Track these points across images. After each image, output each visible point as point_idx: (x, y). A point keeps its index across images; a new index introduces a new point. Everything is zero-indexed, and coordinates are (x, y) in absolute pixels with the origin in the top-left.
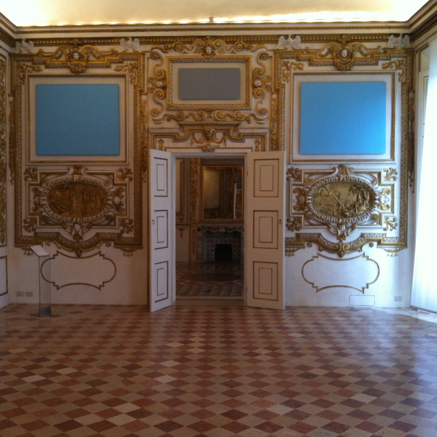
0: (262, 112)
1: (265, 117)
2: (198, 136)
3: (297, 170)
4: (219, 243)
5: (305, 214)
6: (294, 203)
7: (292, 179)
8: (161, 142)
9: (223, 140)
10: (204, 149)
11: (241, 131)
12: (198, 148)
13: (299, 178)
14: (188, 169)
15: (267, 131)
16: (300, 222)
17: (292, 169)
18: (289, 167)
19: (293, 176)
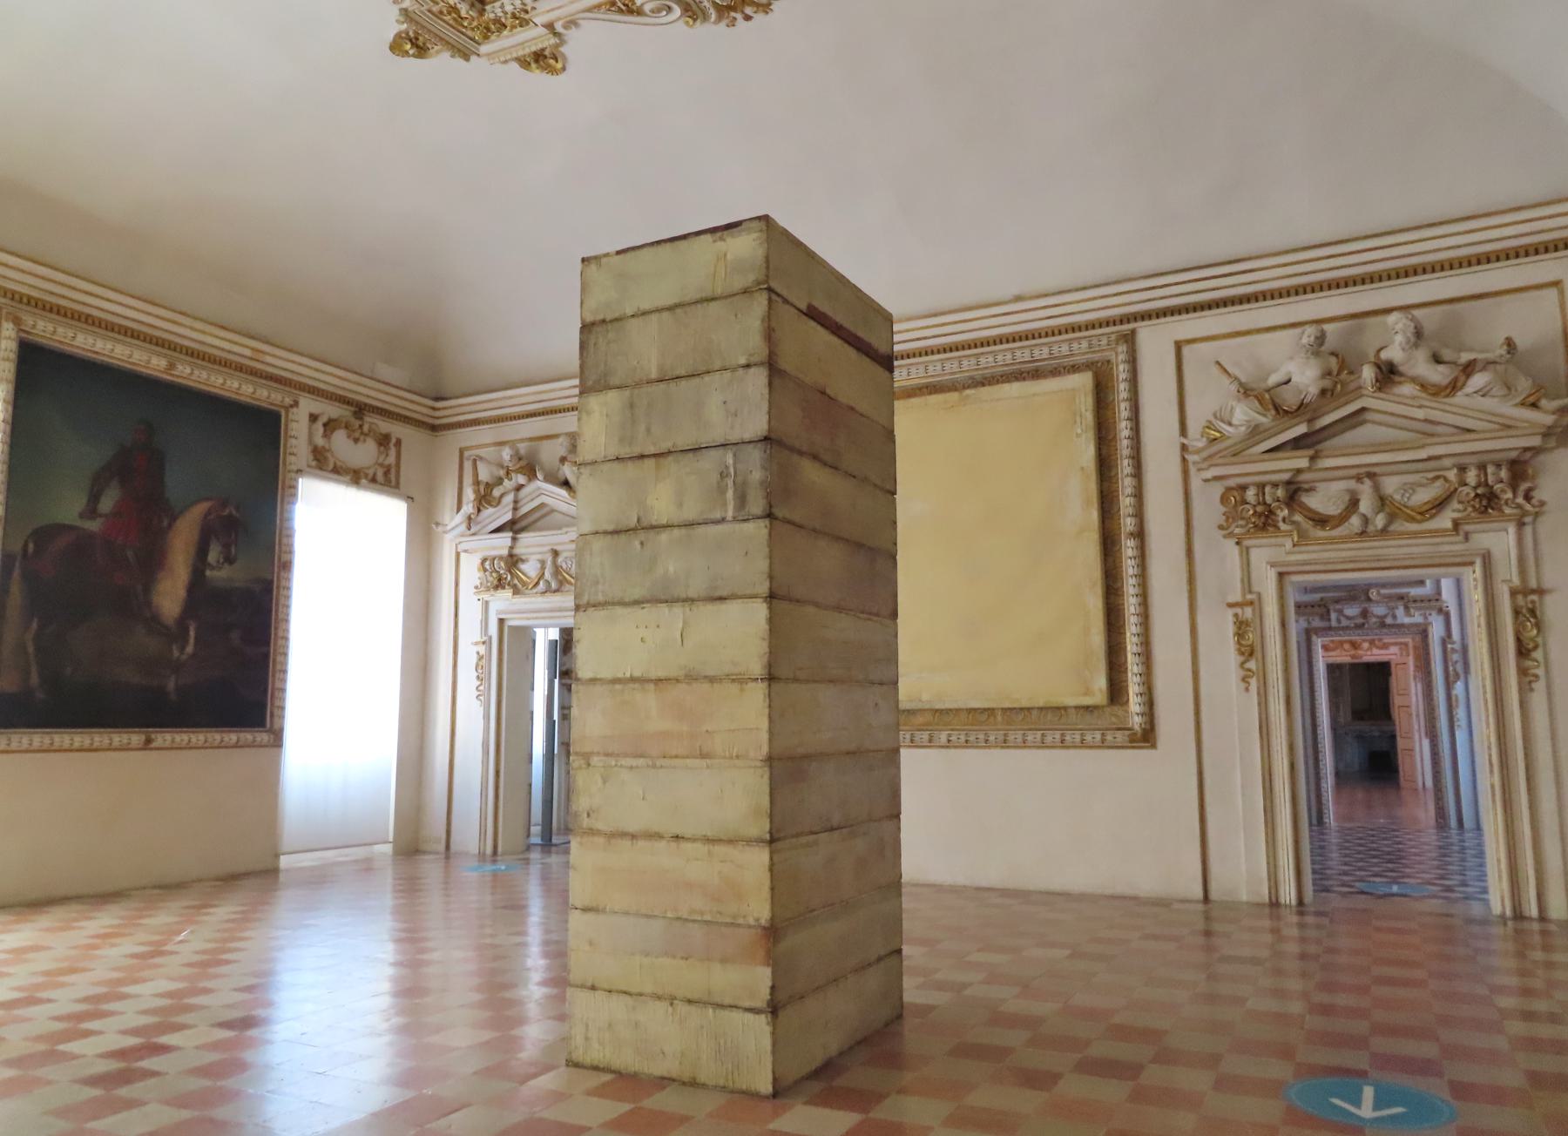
9: (1370, 649)
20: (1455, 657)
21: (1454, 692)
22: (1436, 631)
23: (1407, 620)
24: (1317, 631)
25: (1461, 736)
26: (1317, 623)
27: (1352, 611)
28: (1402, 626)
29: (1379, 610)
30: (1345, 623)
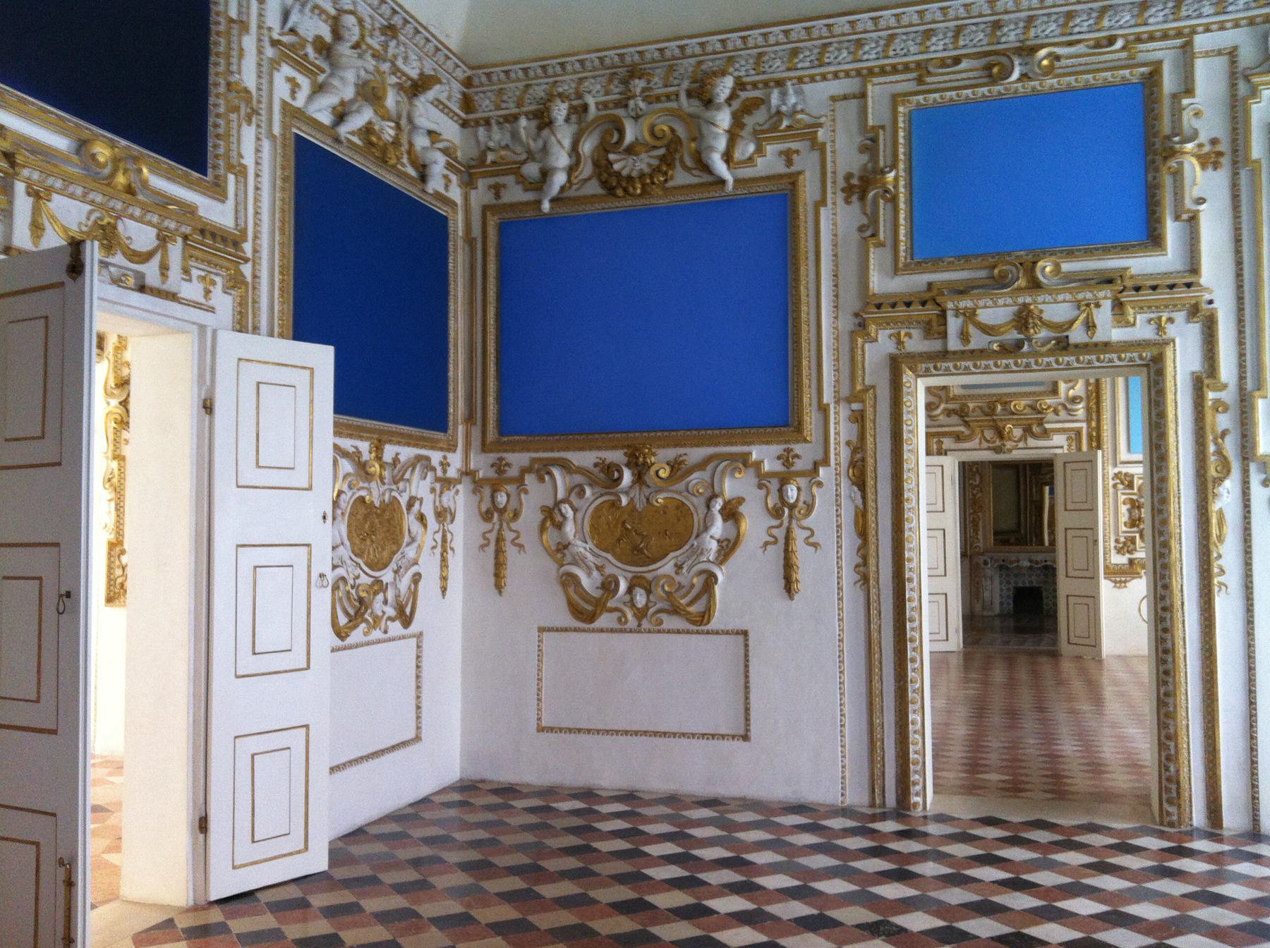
0: (1074, 400)
1: (1080, 406)
2: (989, 434)
3: (1126, 474)
4: (1020, 585)
6: (1124, 516)
7: (1120, 487)
9: (1023, 438)
11: (1047, 426)
12: (989, 449)
13: (1130, 486)
15: (1084, 425)
17: (1120, 473)
18: (1116, 470)
19: (1122, 483)
20: (1224, 421)
21: (1215, 506)
22: (1183, 359)
23: (1117, 335)
24: (914, 360)
25: (1226, 608)
26: (916, 343)
27: (996, 312)
28: (1106, 346)
29: (1056, 310)
30: (978, 340)
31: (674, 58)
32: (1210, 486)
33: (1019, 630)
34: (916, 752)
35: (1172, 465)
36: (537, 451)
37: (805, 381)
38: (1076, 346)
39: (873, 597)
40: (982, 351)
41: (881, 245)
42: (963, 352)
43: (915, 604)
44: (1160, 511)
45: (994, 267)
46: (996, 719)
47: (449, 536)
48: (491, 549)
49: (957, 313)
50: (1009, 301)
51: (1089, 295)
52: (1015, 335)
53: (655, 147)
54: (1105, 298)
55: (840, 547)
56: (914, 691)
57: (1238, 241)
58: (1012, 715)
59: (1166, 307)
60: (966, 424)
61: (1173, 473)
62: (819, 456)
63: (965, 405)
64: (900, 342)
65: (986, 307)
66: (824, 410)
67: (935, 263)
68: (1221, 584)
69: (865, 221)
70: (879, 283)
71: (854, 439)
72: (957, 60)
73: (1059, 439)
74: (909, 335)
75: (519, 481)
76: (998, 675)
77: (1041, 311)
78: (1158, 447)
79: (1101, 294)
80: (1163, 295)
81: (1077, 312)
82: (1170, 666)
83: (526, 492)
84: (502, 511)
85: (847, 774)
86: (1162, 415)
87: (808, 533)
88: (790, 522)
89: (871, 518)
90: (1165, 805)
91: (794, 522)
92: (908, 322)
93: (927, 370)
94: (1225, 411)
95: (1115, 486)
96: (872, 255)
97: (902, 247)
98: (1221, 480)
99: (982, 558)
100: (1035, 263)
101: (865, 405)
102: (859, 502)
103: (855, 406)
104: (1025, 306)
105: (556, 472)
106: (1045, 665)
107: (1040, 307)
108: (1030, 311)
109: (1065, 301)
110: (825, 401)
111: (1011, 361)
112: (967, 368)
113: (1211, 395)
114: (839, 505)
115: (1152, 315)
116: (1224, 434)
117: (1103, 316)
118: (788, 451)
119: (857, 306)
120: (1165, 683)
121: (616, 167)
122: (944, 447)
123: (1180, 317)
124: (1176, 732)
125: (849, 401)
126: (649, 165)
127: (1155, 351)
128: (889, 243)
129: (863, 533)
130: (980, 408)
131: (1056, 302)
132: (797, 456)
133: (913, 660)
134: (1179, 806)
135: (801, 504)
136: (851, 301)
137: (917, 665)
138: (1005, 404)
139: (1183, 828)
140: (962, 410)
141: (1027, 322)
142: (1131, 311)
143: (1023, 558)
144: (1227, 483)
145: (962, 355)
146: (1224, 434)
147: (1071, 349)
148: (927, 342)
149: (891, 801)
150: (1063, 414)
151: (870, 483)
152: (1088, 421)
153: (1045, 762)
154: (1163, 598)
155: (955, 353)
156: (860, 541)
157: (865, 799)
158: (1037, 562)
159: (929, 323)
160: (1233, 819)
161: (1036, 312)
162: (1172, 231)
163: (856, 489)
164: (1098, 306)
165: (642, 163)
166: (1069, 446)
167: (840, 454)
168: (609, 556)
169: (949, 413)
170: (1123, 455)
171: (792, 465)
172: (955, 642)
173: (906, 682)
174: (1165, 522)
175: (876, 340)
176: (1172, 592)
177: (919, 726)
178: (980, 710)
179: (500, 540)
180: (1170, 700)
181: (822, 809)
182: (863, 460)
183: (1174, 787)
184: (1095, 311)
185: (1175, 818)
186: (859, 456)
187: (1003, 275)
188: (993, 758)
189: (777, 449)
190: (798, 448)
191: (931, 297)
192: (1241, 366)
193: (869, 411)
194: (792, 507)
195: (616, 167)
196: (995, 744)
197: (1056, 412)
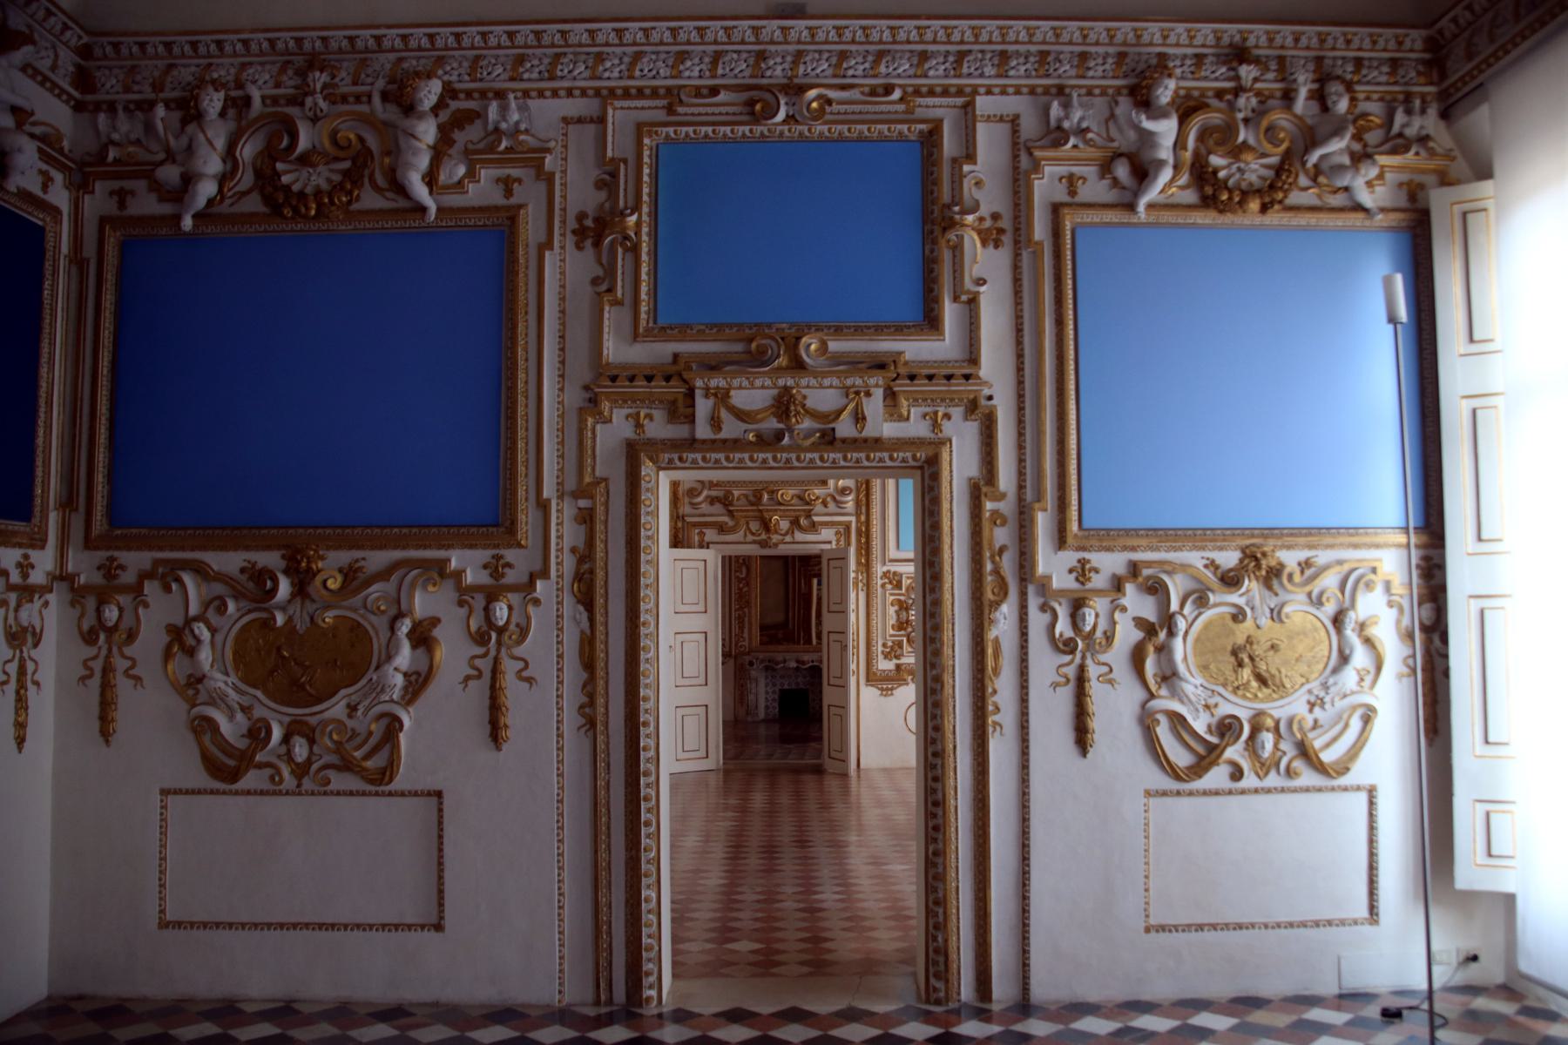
0: (844, 491)
2: (754, 526)
3: (895, 573)
5: (908, 636)
6: (892, 620)
7: (889, 586)
8: (702, 534)
9: (790, 532)
10: (764, 544)
11: (816, 519)
12: (754, 542)
13: (899, 585)
14: (736, 571)
15: (853, 519)
16: (901, 647)
20: (1001, 536)
21: (992, 634)
22: (960, 464)
23: (889, 430)
24: (655, 448)
25: (1001, 751)
26: (658, 427)
27: (752, 395)
28: (877, 443)
29: (822, 397)
30: (731, 428)
31: (367, 50)
32: (986, 611)
33: (785, 739)
34: (649, 936)
35: (947, 586)
36: (161, 549)
37: (521, 469)
38: (844, 441)
39: (601, 746)
40: (736, 441)
41: (617, 303)
42: (714, 441)
43: (652, 753)
44: (933, 640)
45: (751, 340)
46: (754, 861)
47: (30, 666)
48: (96, 682)
49: (707, 392)
50: (768, 382)
51: (859, 382)
52: (773, 424)
53: (337, 159)
54: (877, 386)
55: (560, 682)
56: (648, 862)
57: (1019, 330)
58: (770, 851)
59: (943, 400)
60: (731, 513)
61: (947, 596)
62: (538, 566)
63: (729, 492)
64: (638, 425)
65: (740, 388)
66: (544, 506)
67: (683, 331)
68: (995, 723)
69: (600, 273)
70: (615, 349)
71: (581, 545)
72: (714, 91)
73: (827, 534)
74: (650, 417)
75: (137, 590)
76: (758, 799)
77: (805, 397)
78: (932, 564)
79: (872, 381)
80: (939, 387)
81: (845, 401)
82: (940, 821)
83: (146, 605)
84: (111, 631)
85: (566, 967)
86: (936, 526)
87: (521, 665)
88: (498, 651)
89: (600, 646)
90: (933, 981)
91: (503, 650)
92: (650, 400)
93: (671, 461)
94: (1004, 524)
95: (883, 586)
96: (606, 315)
97: (644, 308)
98: (998, 604)
99: (747, 658)
100: (798, 339)
101: (594, 503)
102: (585, 624)
103: (583, 503)
104: (787, 389)
105: (187, 579)
106: (809, 780)
107: (804, 391)
108: (792, 396)
109: (831, 387)
110: (545, 495)
111: (769, 456)
112: (717, 461)
113: (989, 506)
114: (561, 630)
115: (928, 409)
116: (1002, 550)
117: (874, 406)
118: (498, 558)
119: (587, 377)
120: (935, 840)
121: (285, 179)
122: (707, 539)
123: (957, 412)
124: (945, 896)
125: (576, 495)
126: (329, 180)
127: (931, 452)
128: (628, 301)
129: (589, 663)
130: (746, 496)
131: (821, 387)
132: (508, 565)
133: (648, 824)
134: (947, 981)
135: (512, 627)
136: (580, 371)
137: (653, 829)
138: (772, 492)
139: (952, 1005)
140: (726, 497)
141: (788, 409)
142: (905, 403)
143: (789, 657)
144: (1005, 608)
145: (713, 445)
146: (1002, 550)
147: (838, 444)
148: (670, 427)
149: (620, 994)
150: (832, 507)
151: (599, 601)
152: (858, 515)
153: (804, 920)
154: (934, 741)
155: (704, 441)
156: (585, 675)
157: (589, 996)
158: (803, 663)
159: (674, 402)
160: (1003, 990)
161: (799, 398)
162: (950, 312)
163: (581, 608)
164: (868, 394)
165: (320, 178)
166: (838, 541)
167: (563, 564)
168: (259, 694)
169: (712, 501)
170: (893, 553)
171: (503, 575)
172: (716, 759)
173: (639, 850)
174: (937, 653)
175: (610, 421)
176: (943, 736)
177: (653, 904)
178: (736, 851)
179: (107, 670)
180: (940, 860)
181: (534, 1013)
182: (592, 572)
183: (941, 959)
184: (864, 400)
185: (942, 994)
186: (586, 566)
187: (762, 351)
188: (746, 918)
189: (483, 555)
190: (510, 555)
191: (676, 371)
192: (1021, 474)
193: (600, 509)
194: (501, 631)
195: (285, 179)
196: (749, 895)
197: (825, 504)
